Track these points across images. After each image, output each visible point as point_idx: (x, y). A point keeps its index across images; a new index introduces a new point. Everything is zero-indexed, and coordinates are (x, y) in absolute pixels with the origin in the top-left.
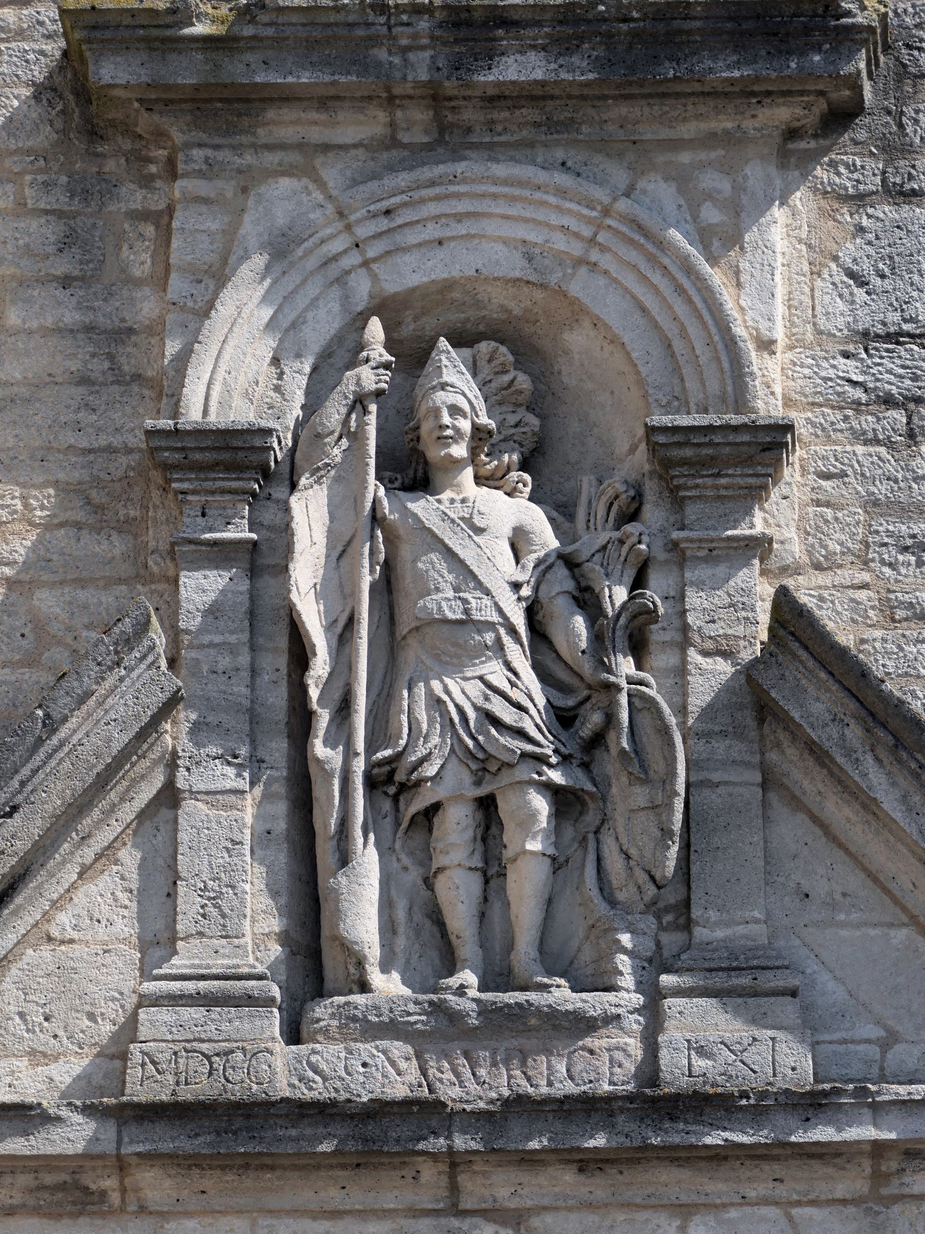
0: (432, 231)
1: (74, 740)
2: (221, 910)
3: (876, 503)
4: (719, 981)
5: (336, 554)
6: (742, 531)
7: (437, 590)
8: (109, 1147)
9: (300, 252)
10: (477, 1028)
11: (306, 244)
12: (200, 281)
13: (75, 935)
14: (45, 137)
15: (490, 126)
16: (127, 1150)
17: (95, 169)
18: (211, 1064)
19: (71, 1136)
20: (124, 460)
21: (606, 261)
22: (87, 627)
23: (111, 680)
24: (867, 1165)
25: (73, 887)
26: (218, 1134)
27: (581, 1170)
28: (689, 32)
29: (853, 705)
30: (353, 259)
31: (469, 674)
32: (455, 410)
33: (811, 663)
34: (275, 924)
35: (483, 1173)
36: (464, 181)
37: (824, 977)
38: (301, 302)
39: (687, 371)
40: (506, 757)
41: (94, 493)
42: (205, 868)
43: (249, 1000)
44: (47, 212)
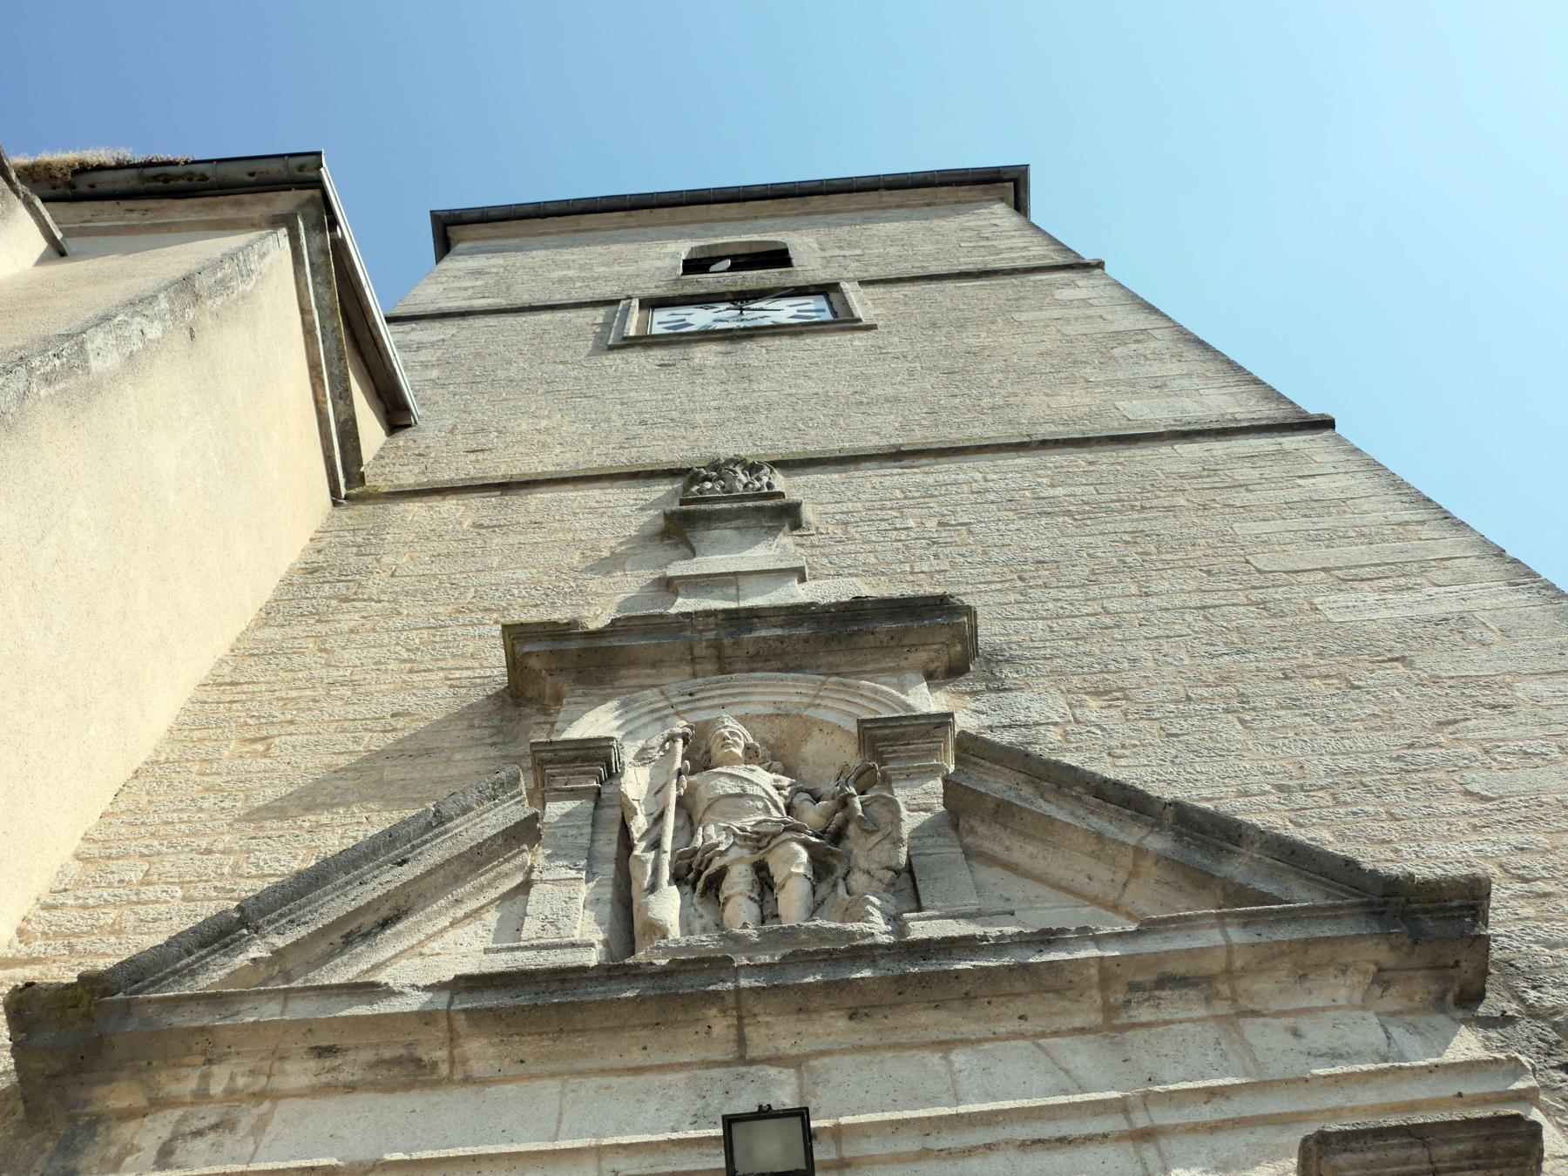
1: (457, 831)
24: (1096, 995)
25: (445, 929)
27: (852, 1017)
38: (637, 723)
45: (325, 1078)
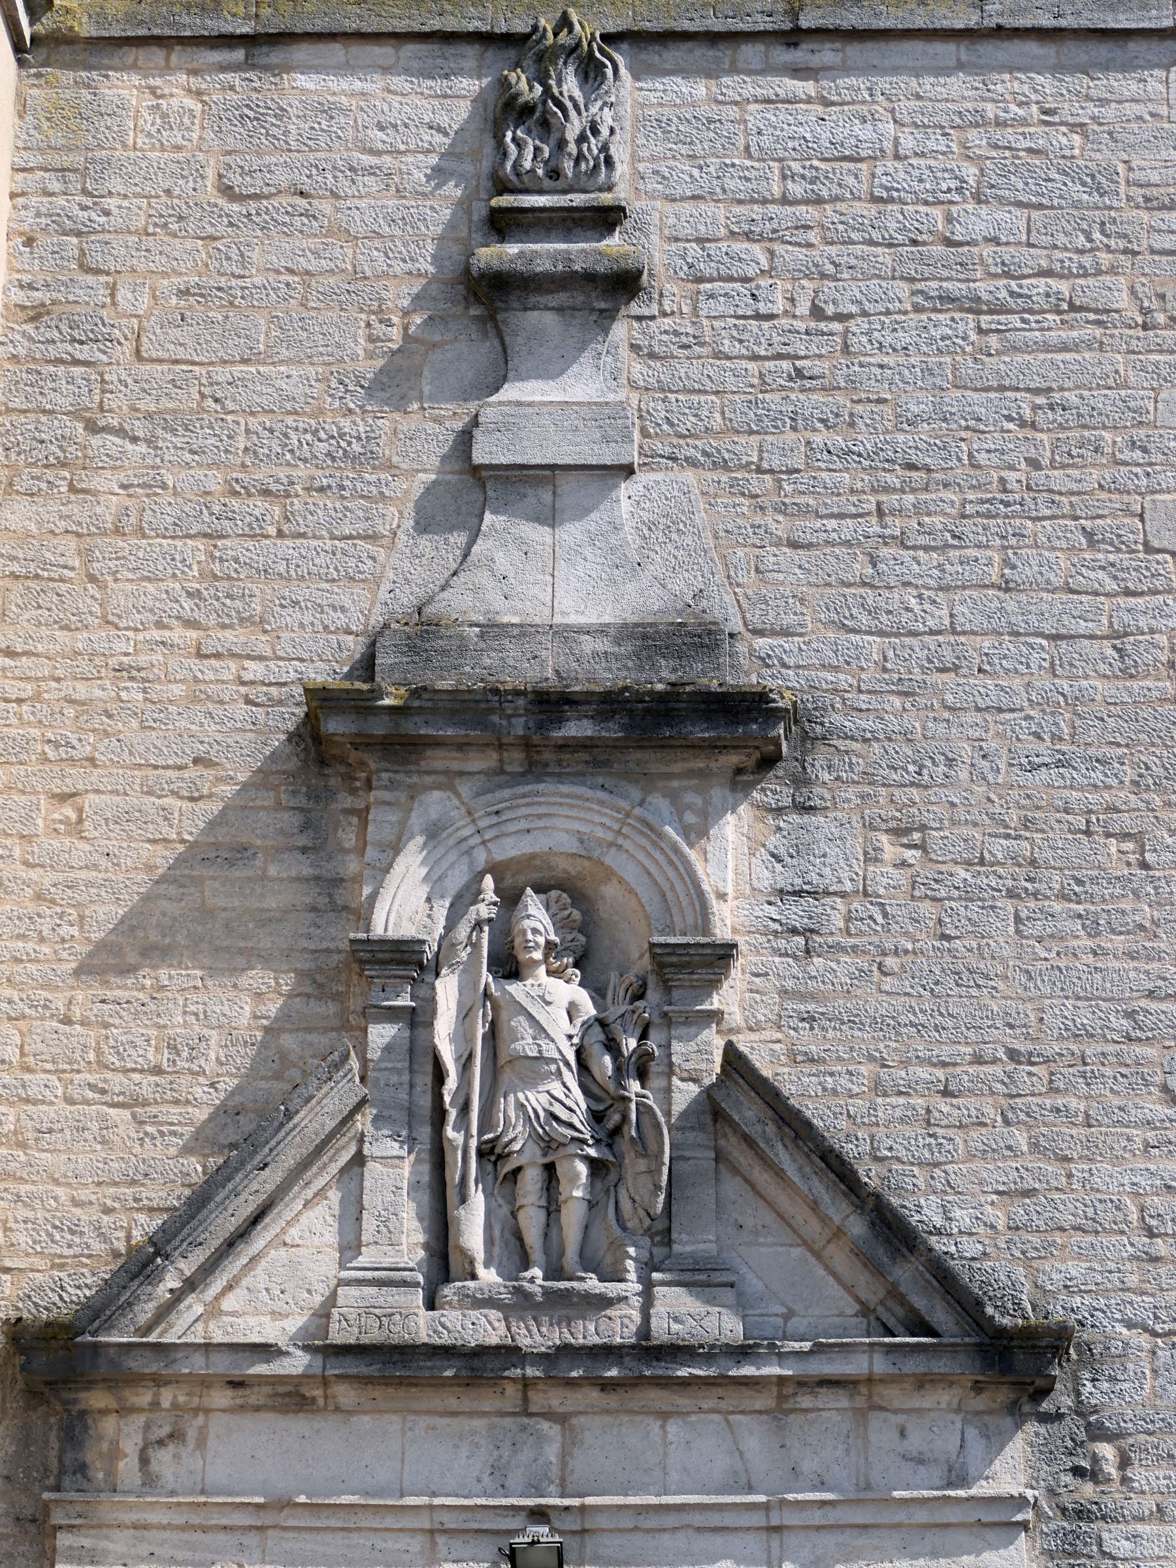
0: (523, 824)
3: (786, 992)
4: (687, 1277)
6: (706, 1007)
8: (318, 1370)
9: (444, 835)
13: (300, 1242)
14: (293, 764)
15: (559, 763)
16: (329, 1372)
20: (336, 957)
21: (627, 844)
22: (312, 1057)
23: (325, 1089)
24: (775, 1390)
25: (300, 1213)
28: (679, 710)
29: (770, 1113)
30: (477, 839)
32: (535, 931)
33: (746, 1087)
34: (421, 1238)
35: (544, 1391)
36: (543, 795)
37: (751, 1277)
38: (445, 865)
39: (674, 911)
40: (562, 1140)
41: (318, 977)
43: (404, 1283)
45: (239, 1401)
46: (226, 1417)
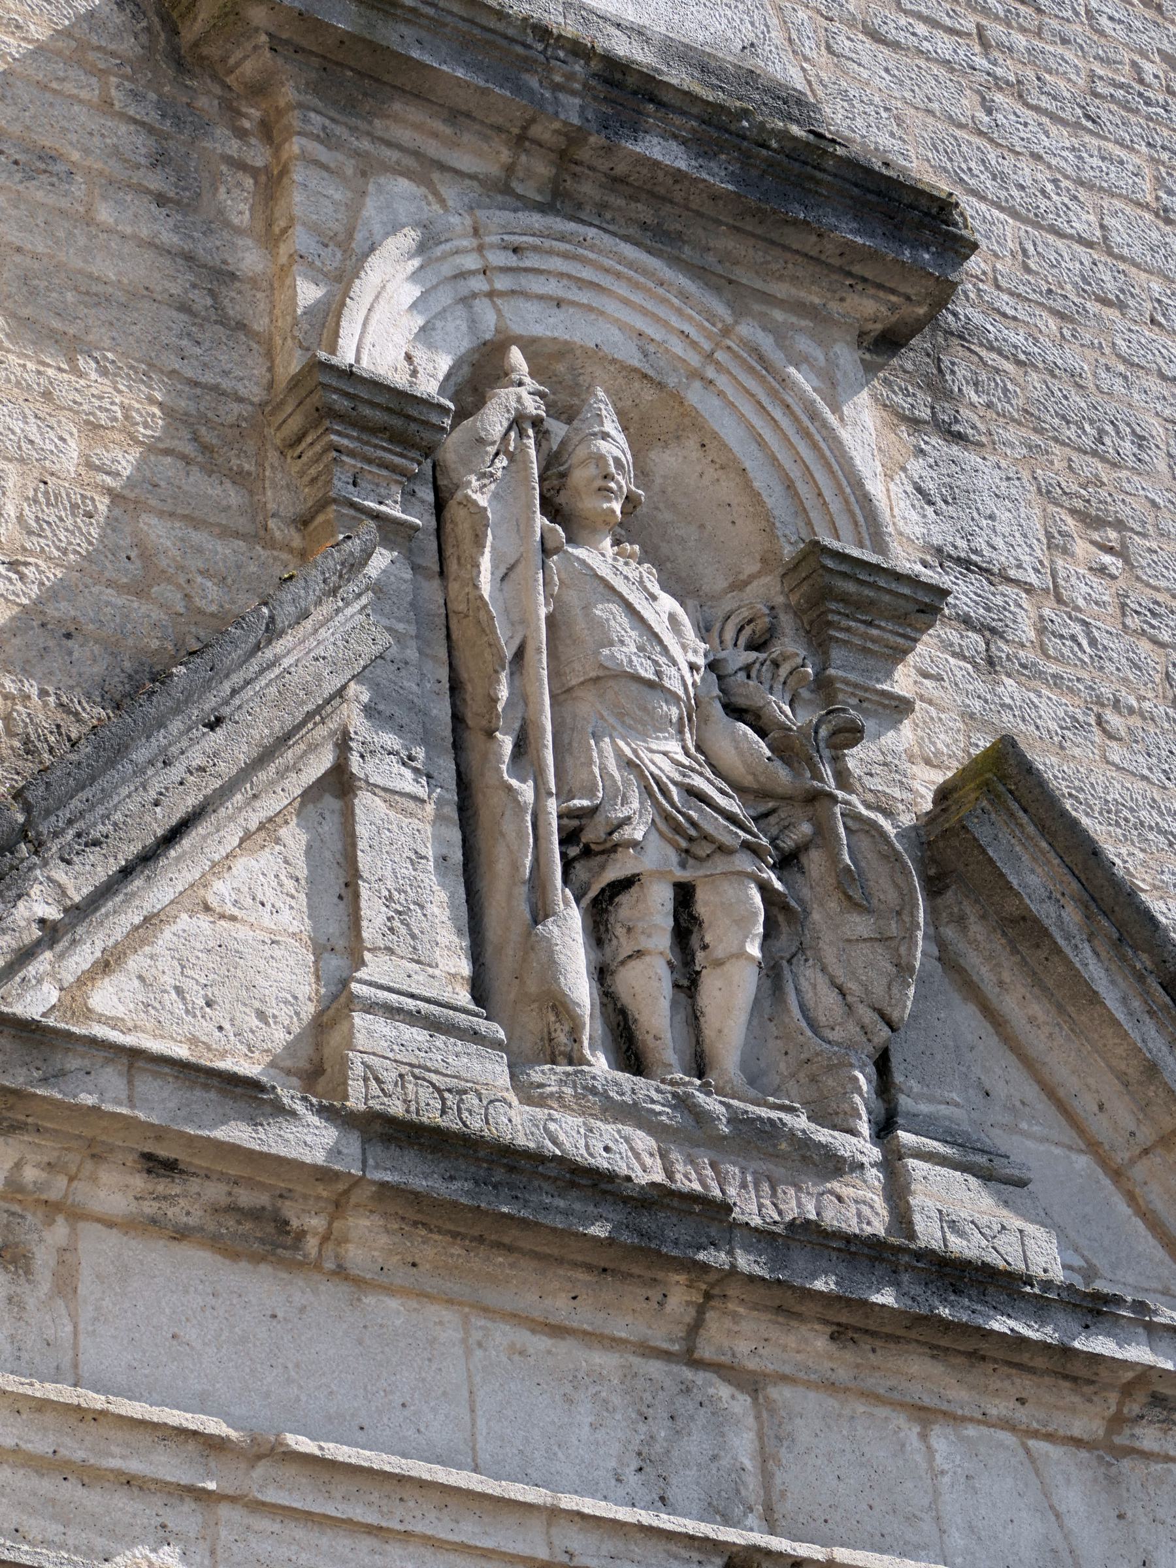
0: (552, 287)
1: (286, 662)
2: (410, 929)
3: (972, 716)
5: (500, 573)
7: (622, 642)
10: (725, 1138)
11: (443, 247)
12: (326, 246)
13: (235, 912)
14: (128, 46)
17: (185, 100)
18: (443, 1099)
19: (308, 1139)
20: (236, 407)
21: (722, 381)
22: (200, 572)
26: (477, 1183)
27: (832, 1337)
28: (818, 182)
31: (654, 747)
33: (1031, 829)
35: (735, 1316)
36: (592, 248)
41: (203, 430)
42: (388, 873)
44: (135, 122)
45: (150, 1208)
46: (113, 1238)
